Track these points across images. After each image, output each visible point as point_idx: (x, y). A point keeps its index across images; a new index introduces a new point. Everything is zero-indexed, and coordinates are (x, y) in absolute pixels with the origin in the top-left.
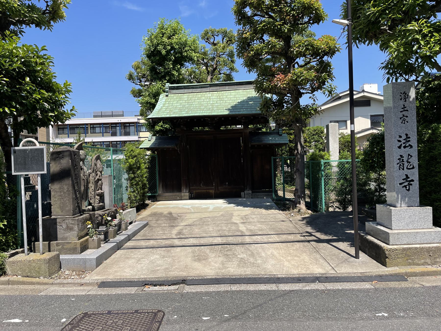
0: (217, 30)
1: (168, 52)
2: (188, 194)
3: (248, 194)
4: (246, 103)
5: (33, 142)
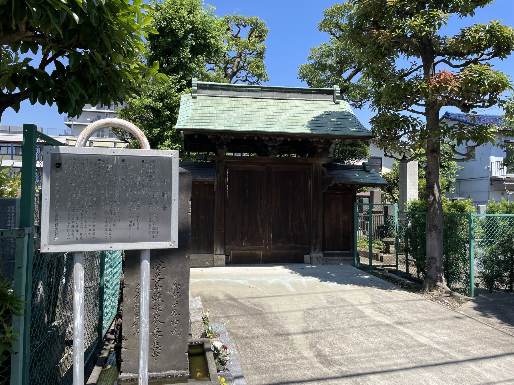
0: (246, 18)
1: (186, 33)
2: (223, 257)
3: (317, 258)
4: (326, 120)
5: (133, 136)
